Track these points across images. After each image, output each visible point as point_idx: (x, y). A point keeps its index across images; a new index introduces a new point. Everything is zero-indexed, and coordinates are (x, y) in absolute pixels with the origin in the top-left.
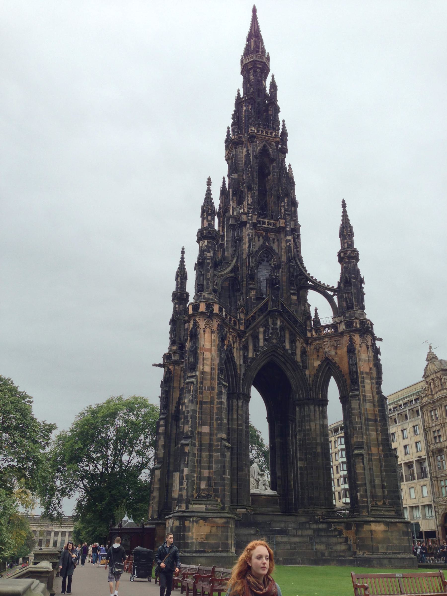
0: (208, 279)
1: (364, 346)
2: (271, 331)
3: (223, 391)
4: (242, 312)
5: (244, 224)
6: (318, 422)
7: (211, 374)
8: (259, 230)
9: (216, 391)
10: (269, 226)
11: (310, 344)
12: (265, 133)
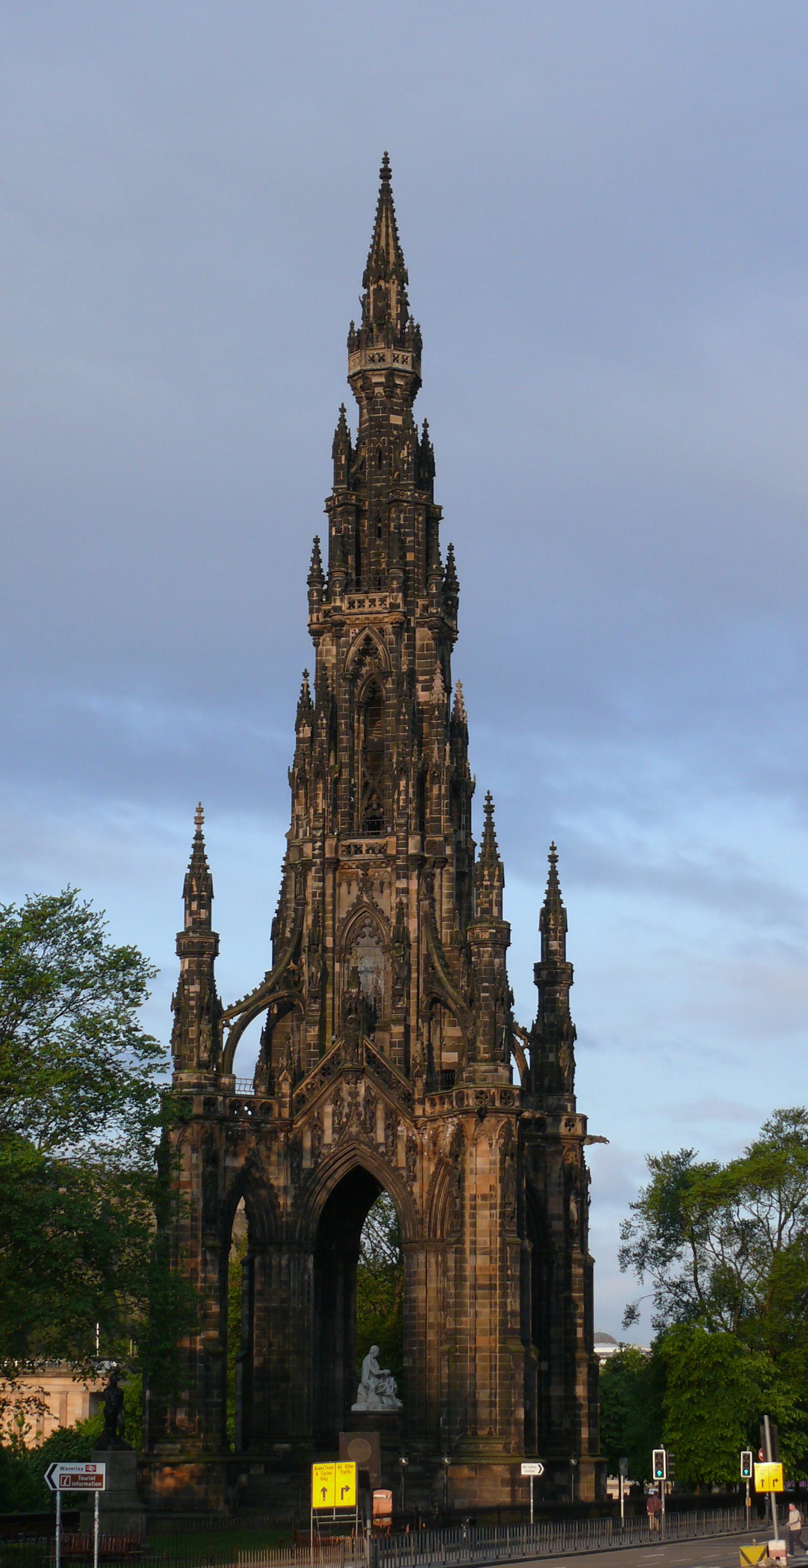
3: (208, 1257)
4: (285, 1079)
5: (307, 865)
6: (432, 1285)
7: (192, 1230)
9: (200, 1258)
12: (367, 603)
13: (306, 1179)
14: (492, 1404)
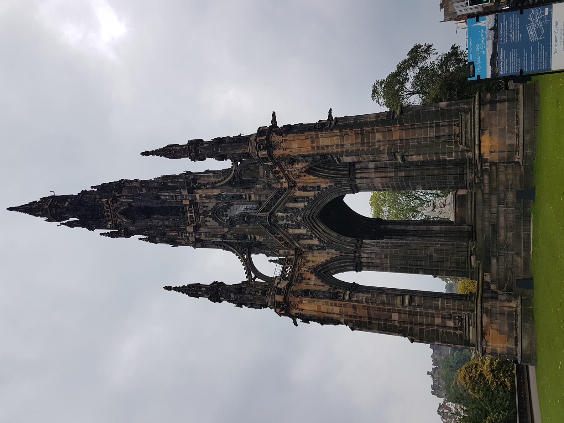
0: (254, 298)
1: (283, 145)
2: (290, 222)
3: (355, 299)
6: (373, 175)
8: (199, 221)
9: (356, 304)
10: (193, 211)
11: (295, 182)
13: (324, 243)
14: (437, 125)
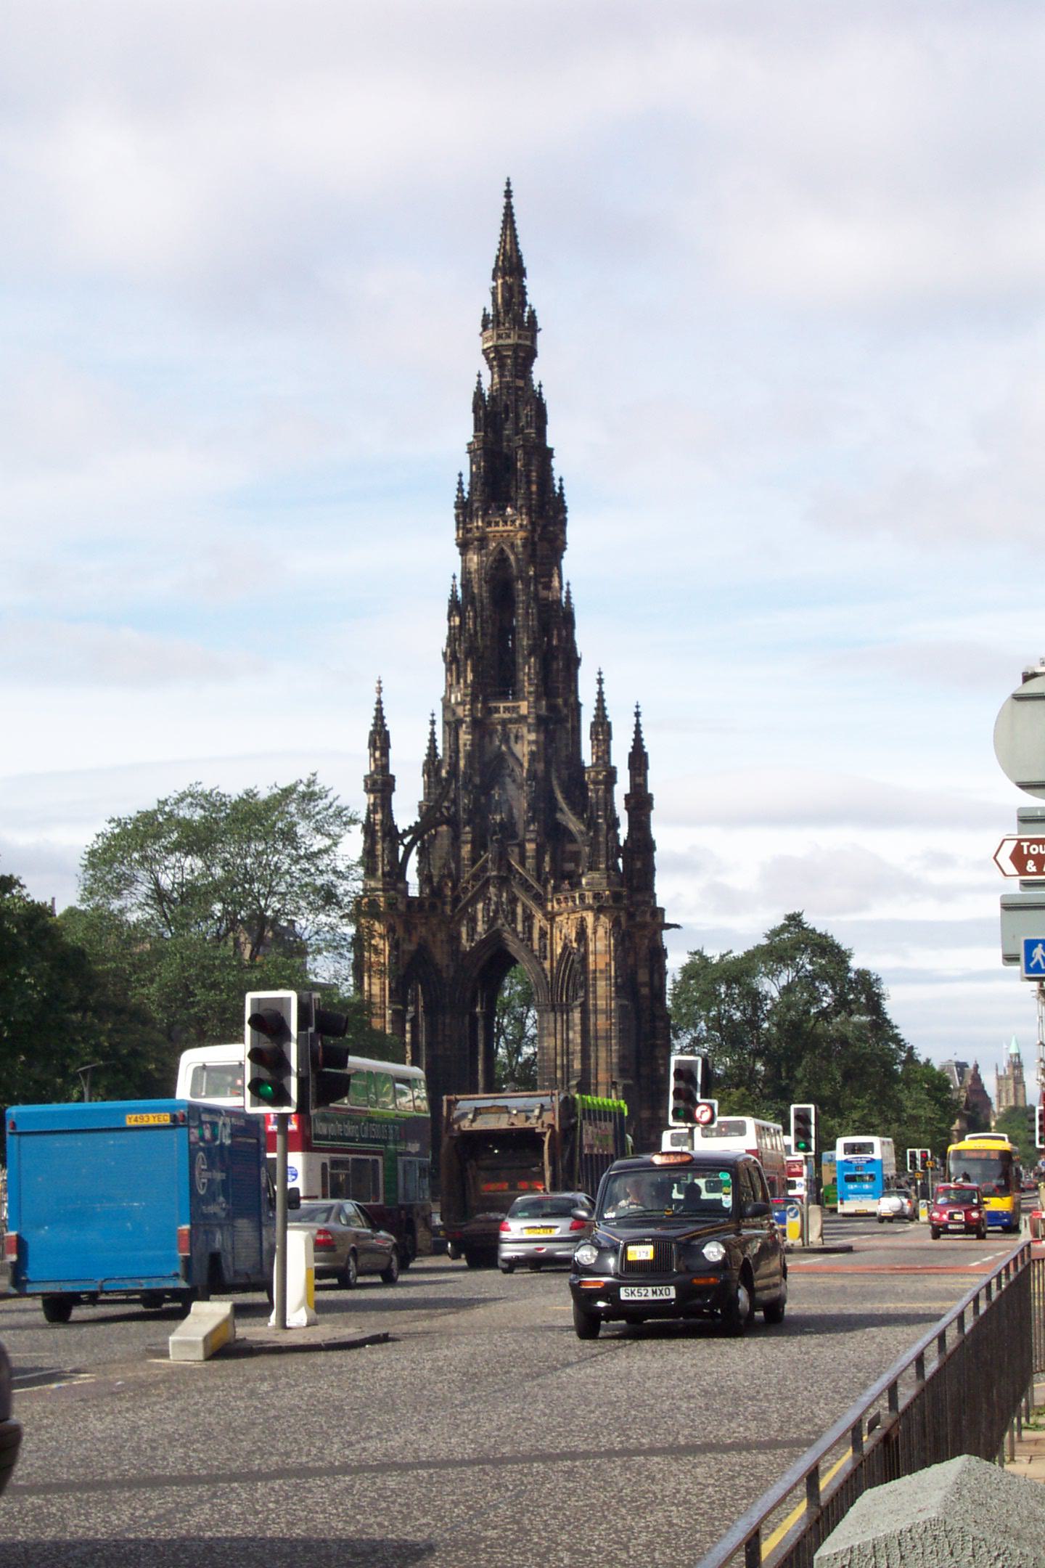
2: (493, 907)
5: (459, 722)
6: (559, 1036)
10: (507, 716)
